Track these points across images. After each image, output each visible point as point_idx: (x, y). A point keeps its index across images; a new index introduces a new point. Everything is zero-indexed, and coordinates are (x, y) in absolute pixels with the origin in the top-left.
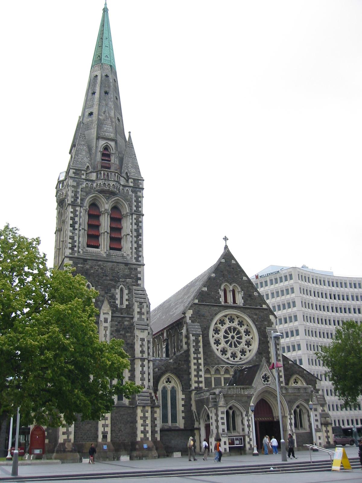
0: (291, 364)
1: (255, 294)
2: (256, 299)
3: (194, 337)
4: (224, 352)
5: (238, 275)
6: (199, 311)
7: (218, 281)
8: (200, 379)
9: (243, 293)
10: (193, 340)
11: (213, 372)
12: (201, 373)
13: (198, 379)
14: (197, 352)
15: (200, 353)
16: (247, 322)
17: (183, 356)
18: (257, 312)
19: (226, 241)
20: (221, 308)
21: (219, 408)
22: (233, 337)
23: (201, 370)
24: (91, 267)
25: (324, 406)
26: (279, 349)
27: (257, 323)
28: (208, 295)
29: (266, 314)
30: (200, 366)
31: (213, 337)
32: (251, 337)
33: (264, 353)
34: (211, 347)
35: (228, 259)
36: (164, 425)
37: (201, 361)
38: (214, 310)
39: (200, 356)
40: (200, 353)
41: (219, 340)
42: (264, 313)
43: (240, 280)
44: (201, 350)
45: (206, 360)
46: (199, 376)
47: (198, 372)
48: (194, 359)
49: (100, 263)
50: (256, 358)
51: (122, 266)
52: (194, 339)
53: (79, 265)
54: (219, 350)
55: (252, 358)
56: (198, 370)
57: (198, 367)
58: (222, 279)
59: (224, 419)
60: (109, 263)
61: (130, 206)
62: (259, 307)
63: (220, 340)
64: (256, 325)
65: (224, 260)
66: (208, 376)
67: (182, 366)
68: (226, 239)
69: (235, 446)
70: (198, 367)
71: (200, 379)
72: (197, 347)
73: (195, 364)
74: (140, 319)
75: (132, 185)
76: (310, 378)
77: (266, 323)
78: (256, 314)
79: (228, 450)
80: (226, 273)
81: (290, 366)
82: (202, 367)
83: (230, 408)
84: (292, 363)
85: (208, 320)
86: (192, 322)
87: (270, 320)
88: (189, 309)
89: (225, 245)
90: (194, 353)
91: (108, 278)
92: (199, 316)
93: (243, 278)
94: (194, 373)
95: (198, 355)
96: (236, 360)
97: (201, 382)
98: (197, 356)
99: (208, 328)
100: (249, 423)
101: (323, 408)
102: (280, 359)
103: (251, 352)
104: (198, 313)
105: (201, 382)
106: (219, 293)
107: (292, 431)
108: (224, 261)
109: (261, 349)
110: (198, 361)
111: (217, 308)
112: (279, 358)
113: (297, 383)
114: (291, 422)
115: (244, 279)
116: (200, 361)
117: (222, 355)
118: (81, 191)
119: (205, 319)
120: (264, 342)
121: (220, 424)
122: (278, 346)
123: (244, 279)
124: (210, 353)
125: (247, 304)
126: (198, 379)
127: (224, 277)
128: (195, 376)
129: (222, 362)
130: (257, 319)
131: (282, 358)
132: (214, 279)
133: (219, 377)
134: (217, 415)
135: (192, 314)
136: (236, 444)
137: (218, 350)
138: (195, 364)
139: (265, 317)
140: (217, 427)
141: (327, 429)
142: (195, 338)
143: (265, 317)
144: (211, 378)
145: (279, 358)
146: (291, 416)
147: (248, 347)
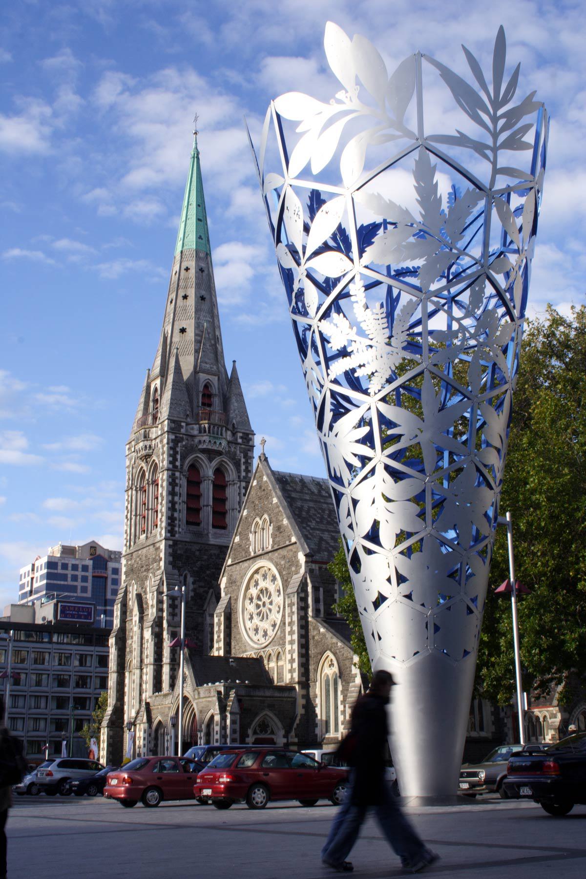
4: (256, 630)
18: (283, 552)
22: (264, 604)
24: (135, 561)
27: (284, 573)
29: (295, 552)
49: (140, 552)
50: (281, 632)
51: (151, 548)
53: (129, 563)
60: (144, 550)
61: (159, 461)
62: (287, 543)
74: (152, 613)
75: (159, 433)
76: (345, 656)
78: (284, 557)
86: (226, 594)
87: (298, 561)
91: (144, 569)
96: (267, 638)
99: (236, 600)
111: (246, 564)
118: (133, 468)
119: (236, 585)
123: (274, 502)
125: (275, 544)
127: (255, 510)
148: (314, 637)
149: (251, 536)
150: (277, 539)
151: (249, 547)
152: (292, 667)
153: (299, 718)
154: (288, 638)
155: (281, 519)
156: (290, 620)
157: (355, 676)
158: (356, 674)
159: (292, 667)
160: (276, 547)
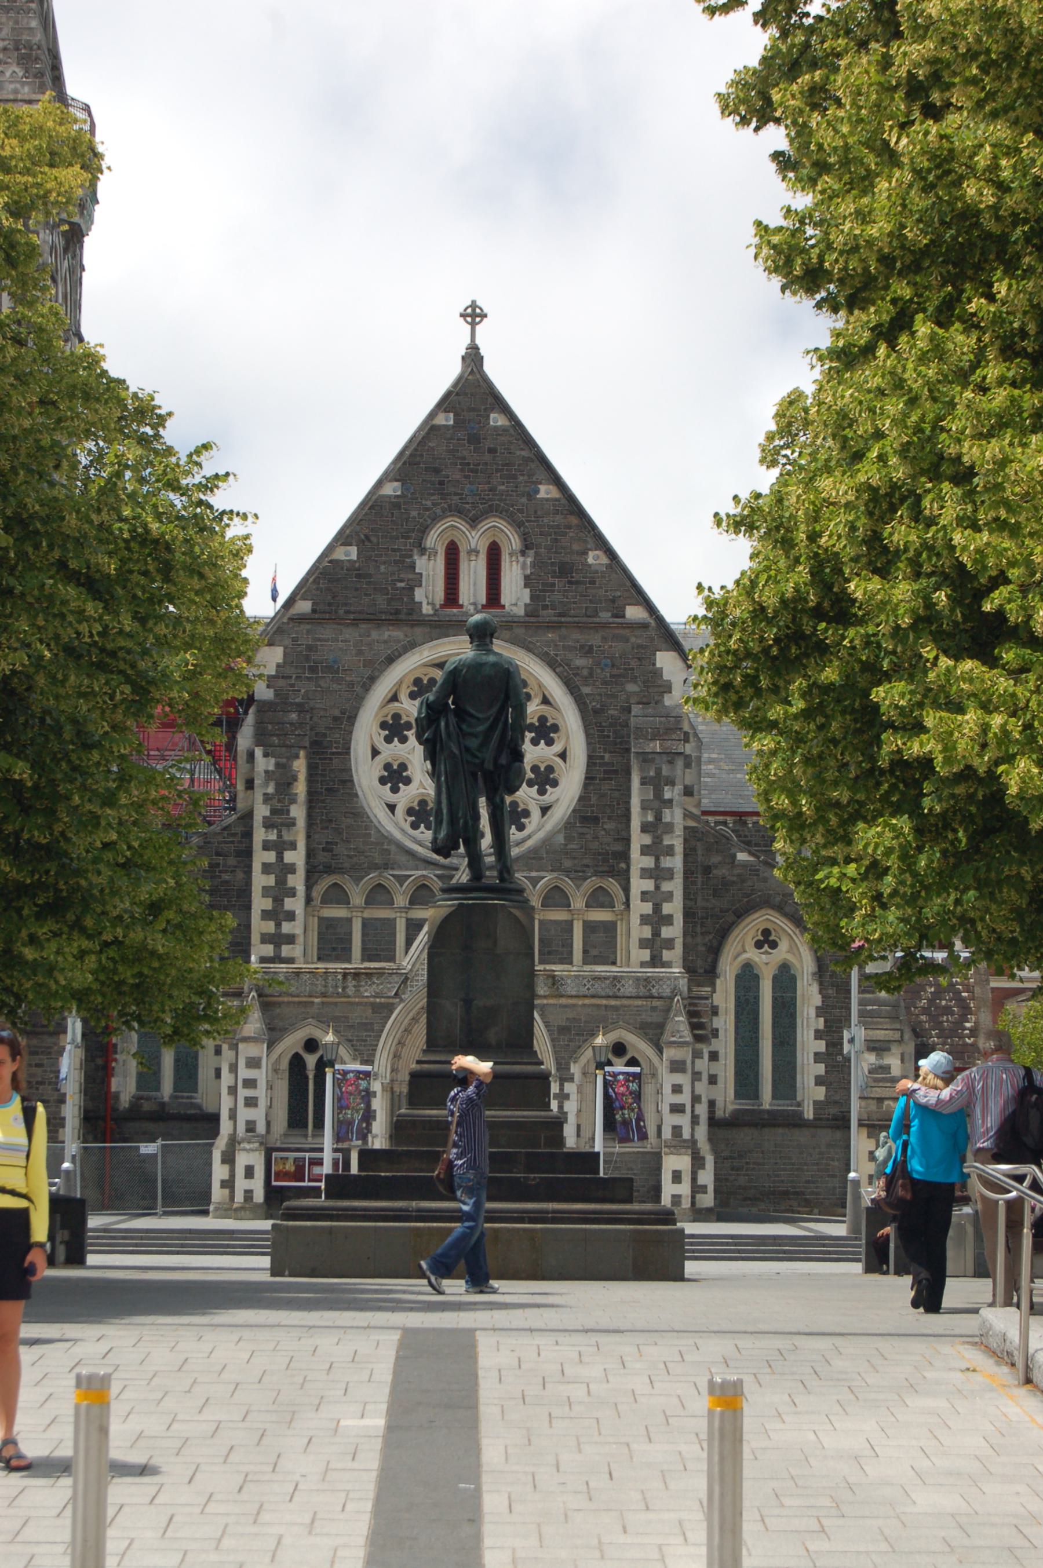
0: (745, 865)
1: (590, 561)
2: (592, 582)
3: (272, 761)
5: (515, 477)
6: (310, 648)
7: (414, 513)
8: (286, 928)
9: (529, 560)
10: (267, 772)
11: (357, 899)
12: (289, 904)
13: (278, 925)
14: (279, 819)
15: (292, 823)
16: (540, 685)
17: (234, 835)
18: (595, 639)
19: (473, 325)
20: (418, 631)
21: (241, 1046)
23: (292, 892)
25: (888, 1049)
26: (671, 801)
27: (586, 690)
28: (358, 576)
29: (639, 646)
30: (289, 876)
31: (375, 753)
32: (557, 748)
33: (610, 818)
34: (357, 795)
35: (471, 410)
36: (141, 1098)
37: (296, 857)
38: (385, 642)
39: (291, 838)
40: (294, 824)
41: (403, 767)
42: (627, 641)
43: (524, 500)
44: (298, 812)
45: (331, 850)
46: (281, 916)
47: (278, 901)
48: (267, 846)
50: (569, 839)
52: (271, 768)
54: (400, 810)
55: (546, 842)
56: (280, 892)
57: (281, 882)
58: (433, 504)
59: (255, 1087)
62: (605, 616)
63: (409, 767)
64: (580, 701)
65: (452, 415)
66: (338, 912)
67: (226, 877)
68: (474, 315)
69: (305, 1184)
70: (281, 882)
71: (286, 928)
72: (279, 801)
73: (267, 868)
77: (631, 688)
79: (259, 1196)
80: (457, 475)
81: (736, 872)
82: (297, 881)
83: (311, 1045)
84: (752, 859)
85: (351, 684)
87: (658, 673)
88: (270, 644)
89: (467, 341)
90: (268, 825)
92: (313, 669)
93: (538, 491)
94: (260, 903)
95: (284, 833)
97: (265, 939)
98: (280, 836)
102: (671, 847)
103: (549, 813)
104: (307, 658)
105: (291, 939)
106: (413, 567)
108: (451, 422)
109: (594, 799)
110: (280, 857)
111: (397, 634)
112: (666, 842)
113: (774, 945)
115: (542, 495)
116: (289, 857)
117: (415, 826)
120: (616, 772)
121: (241, 1102)
122: (666, 788)
123: (542, 495)
124: (349, 820)
125: (545, 607)
126: (278, 925)
127: (444, 496)
128: (266, 915)
129: (403, 859)
130: (591, 675)
131: (681, 840)
132: (395, 504)
133: (388, 919)
134: (234, 1068)
135: (278, 666)
136: (310, 1180)
137: (392, 808)
138: (267, 868)
139: (634, 664)
140: (233, 1115)
142: (278, 765)
143: (634, 664)
144: (349, 920)
145: (666, 842)
146: (566, 1084)
147: (542, 792)
148: (707, 870)
149: (421, 564)
150: (557, 597)
151: (411, 589)
152: (656, 934)
154: (639, 861)
155: (576, 547)
156: (650, 818)
159: (656, 934)
160: (548, 615)
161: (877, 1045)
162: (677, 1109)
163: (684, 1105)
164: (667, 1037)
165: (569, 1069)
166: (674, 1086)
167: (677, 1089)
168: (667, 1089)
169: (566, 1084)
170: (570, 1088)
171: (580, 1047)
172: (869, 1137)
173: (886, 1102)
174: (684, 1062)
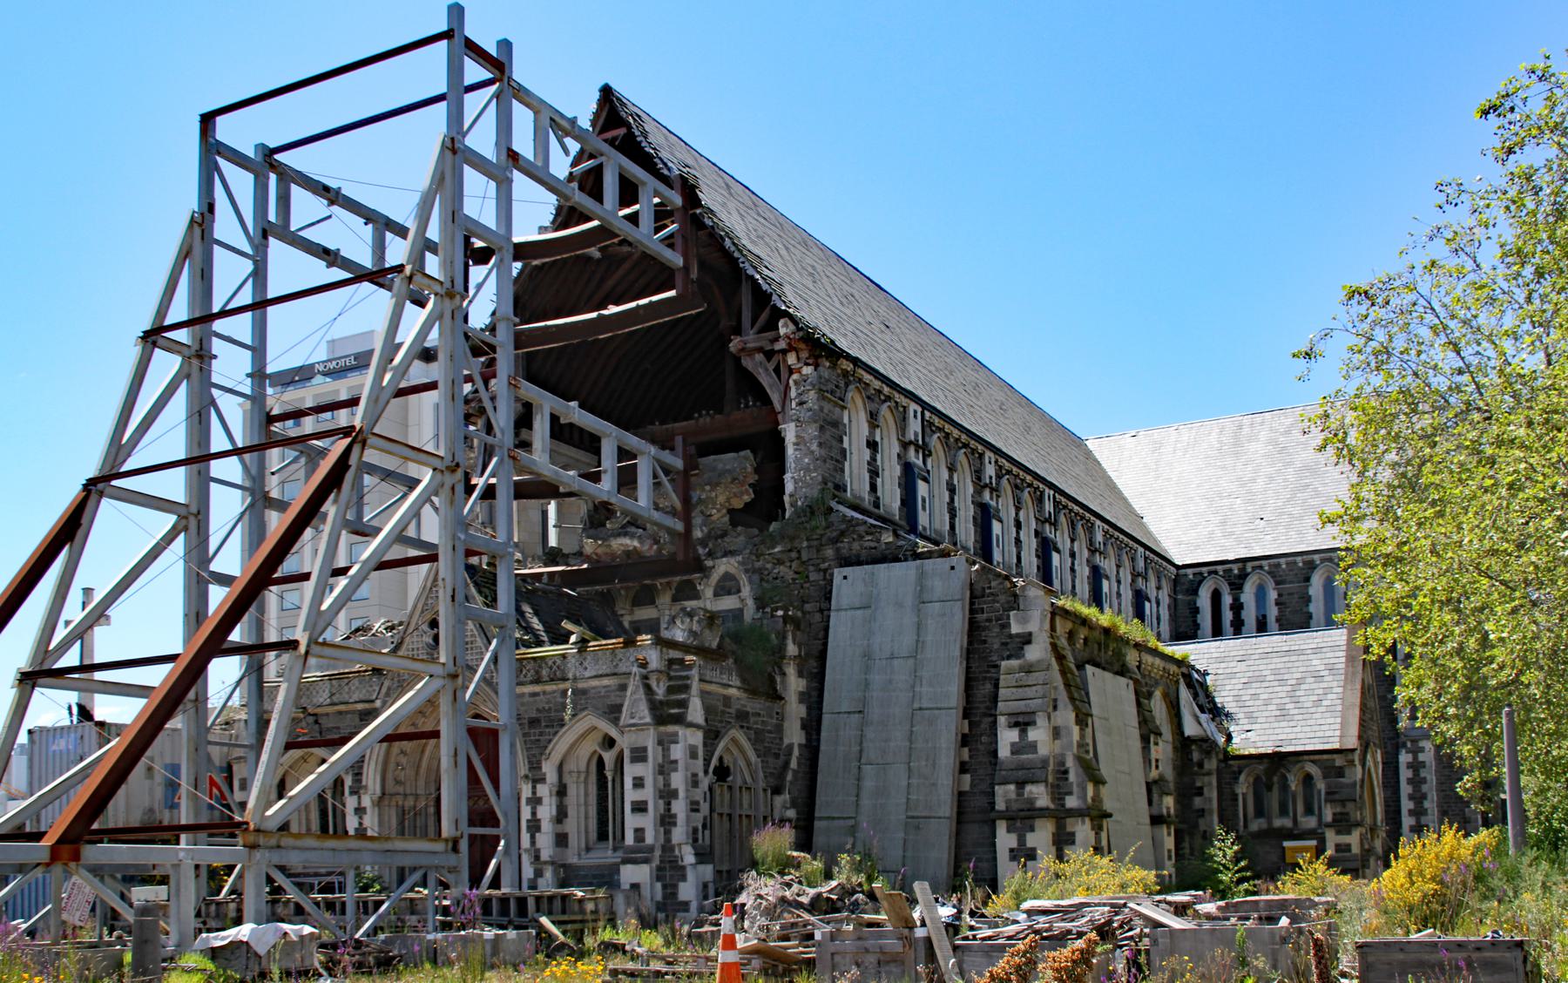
25: (1033, 723)
100: (361, 824)
101: (1023, 732)
107: (537, 857)
114: (534, 814)
141: (1022, 840)
146: (539, 786)
153: (796, 752)
157: (1027, 639)
158: (1030, 634)
161: (1020, 719)
162: (640, 808)
163: (646, 803)
164: (625, 718)
165: (540, 768)
166: (634, 778)
167: (639, 783)
168: (649, 782)
169: (539, 786)
170: (543, 790)
171: (550, 741)
172: (1009, 831)
173: (1029, 788)
174: (645, 749)
